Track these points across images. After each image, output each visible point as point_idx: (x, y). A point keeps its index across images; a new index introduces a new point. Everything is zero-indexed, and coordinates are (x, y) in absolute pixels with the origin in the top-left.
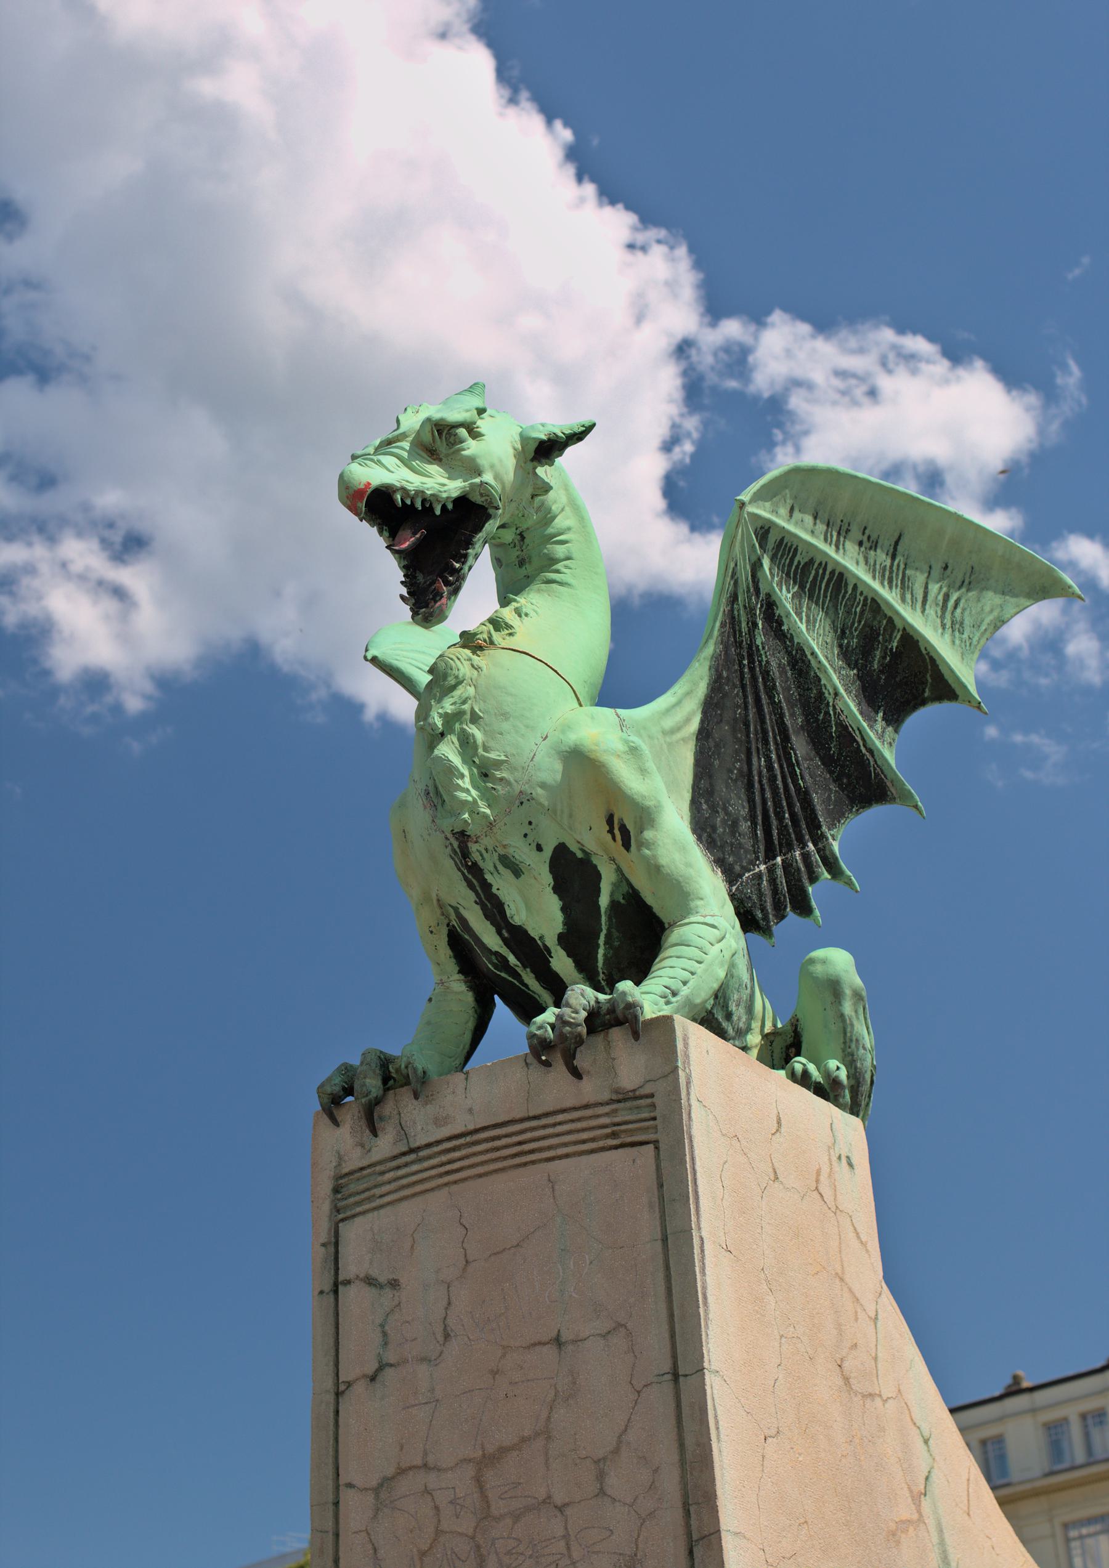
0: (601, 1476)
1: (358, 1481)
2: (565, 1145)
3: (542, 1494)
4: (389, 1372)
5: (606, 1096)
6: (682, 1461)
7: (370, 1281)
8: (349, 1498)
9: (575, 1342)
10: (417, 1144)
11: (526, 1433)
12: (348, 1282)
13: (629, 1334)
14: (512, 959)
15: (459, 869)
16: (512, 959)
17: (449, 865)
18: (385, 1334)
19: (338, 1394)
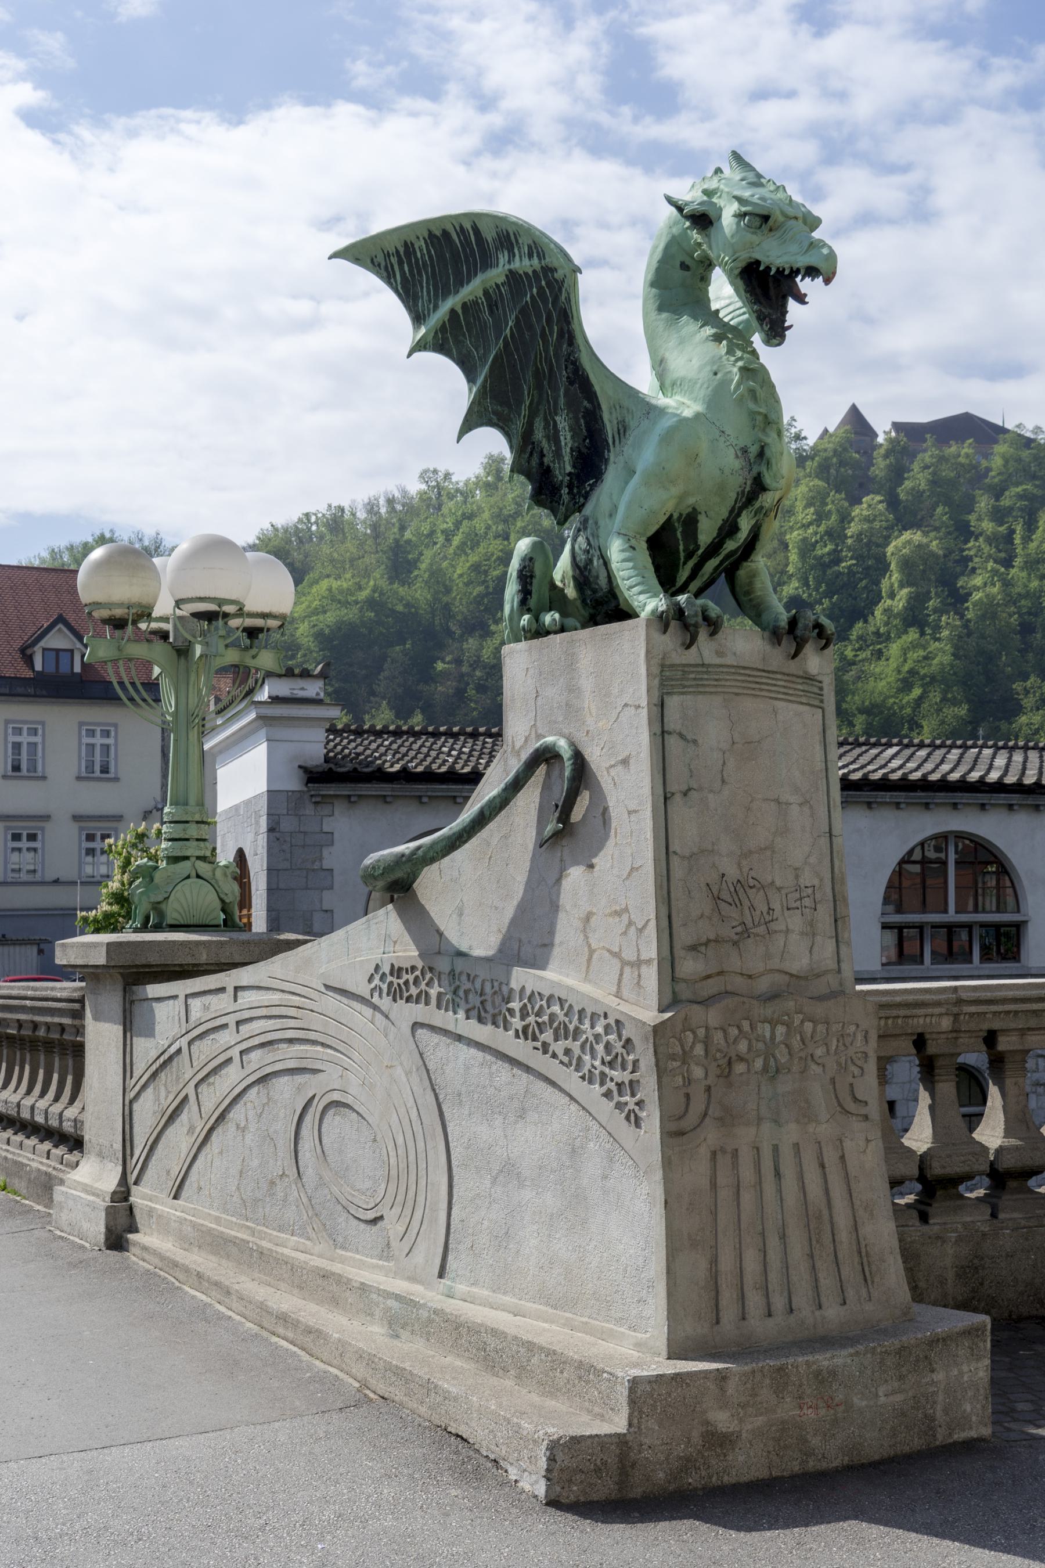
0: (797, 877)
1: (678, 851)
2: (779, 692)
3: (769, 880)
4: (693, 792)
5: (801, 673)
6: (833, 878)
7: (681, 735)
8: (675, 861)
9: (786, 804)
10: (706, 662)
11: (762, 846)
12: (669, 733)
13: (811, 807)
14: (700, 552)
15: (736, 501)
16: (700, 552)
17: (733, 495)
18: (691, 771)
19: (666, 799)
